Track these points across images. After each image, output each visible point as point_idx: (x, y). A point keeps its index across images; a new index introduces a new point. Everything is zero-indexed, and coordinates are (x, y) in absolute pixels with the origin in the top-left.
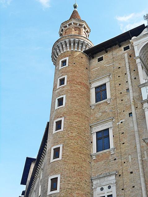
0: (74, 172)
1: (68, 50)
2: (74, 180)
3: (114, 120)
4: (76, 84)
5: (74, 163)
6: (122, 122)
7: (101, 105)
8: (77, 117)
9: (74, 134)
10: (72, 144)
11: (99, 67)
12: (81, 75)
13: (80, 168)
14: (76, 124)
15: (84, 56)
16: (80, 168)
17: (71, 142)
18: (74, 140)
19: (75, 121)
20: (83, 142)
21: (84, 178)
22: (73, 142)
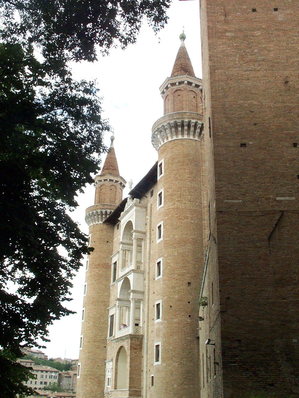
5: (89, 352)
8: (94, 306)
10: (88, 335)
15: (105, 226)
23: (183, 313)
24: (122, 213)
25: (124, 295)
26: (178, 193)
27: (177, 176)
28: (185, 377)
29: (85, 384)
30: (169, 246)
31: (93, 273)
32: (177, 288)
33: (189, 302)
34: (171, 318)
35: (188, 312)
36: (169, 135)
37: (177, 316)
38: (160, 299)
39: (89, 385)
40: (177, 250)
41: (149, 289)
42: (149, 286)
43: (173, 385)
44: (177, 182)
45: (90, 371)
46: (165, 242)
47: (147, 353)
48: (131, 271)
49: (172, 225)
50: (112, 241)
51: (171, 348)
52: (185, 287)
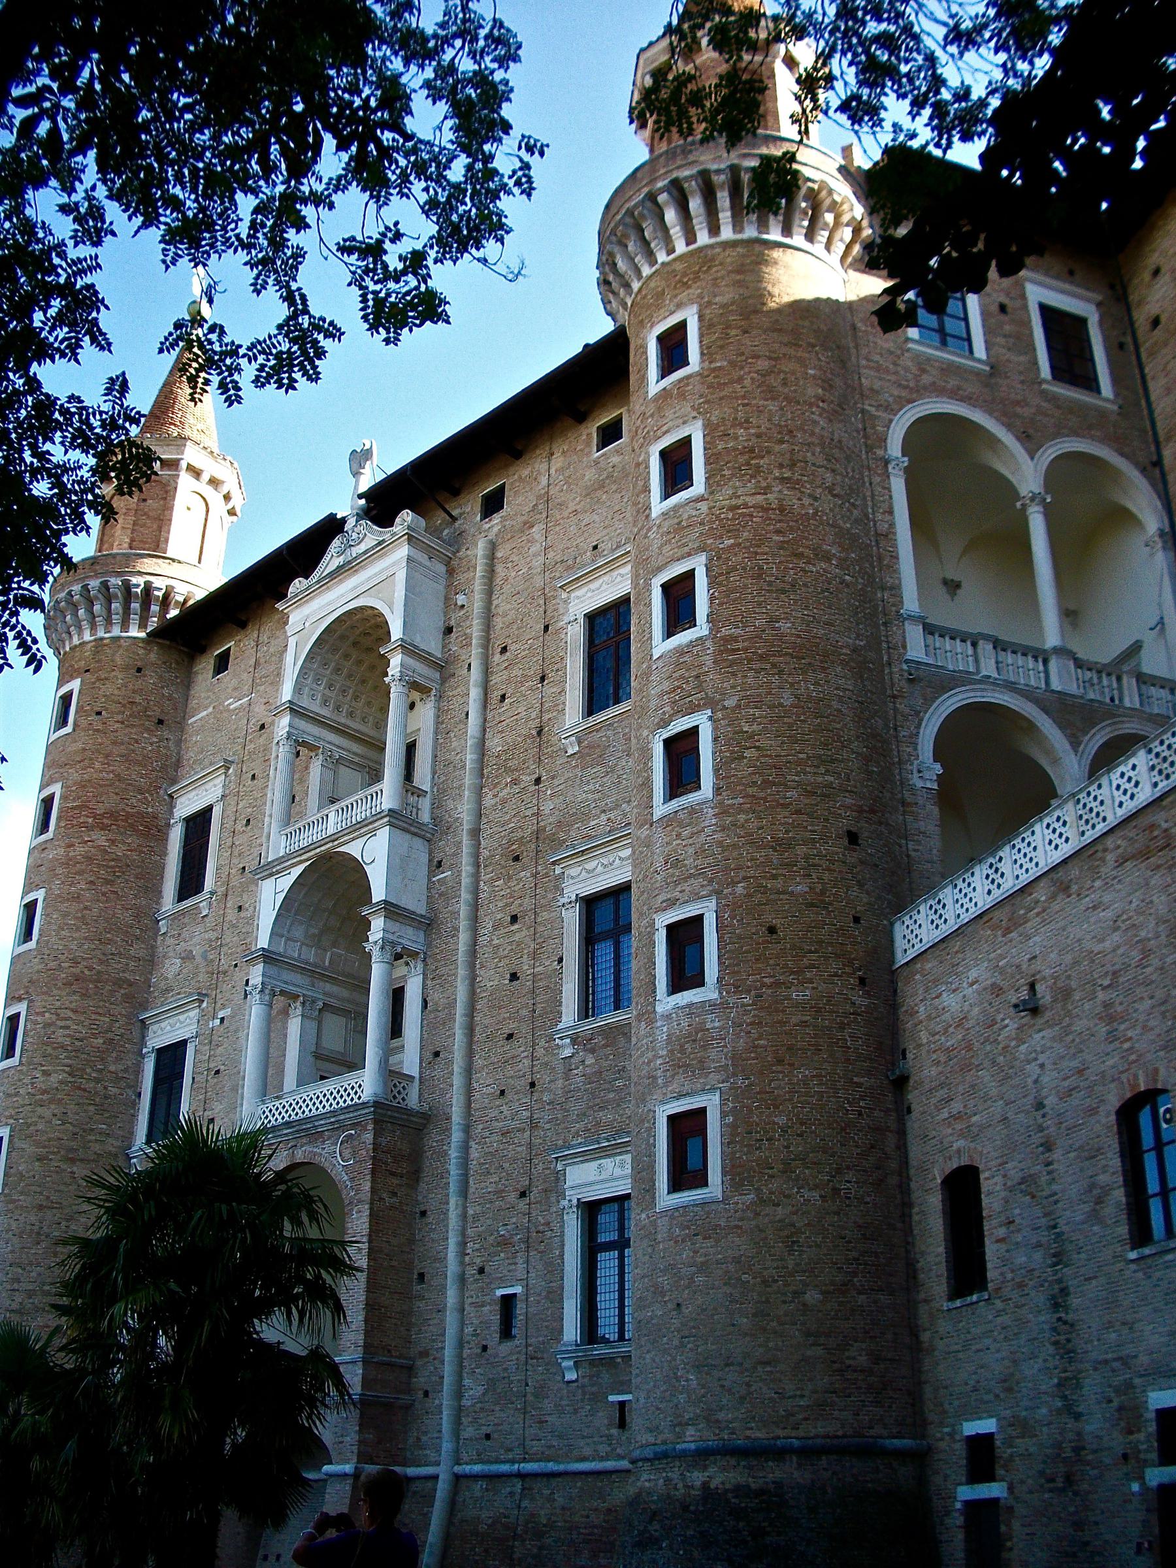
2: (33, 1274)
3: (205, 1005)
4: (90, 828)
6: (222, 1019)
7: (186, 920)
9: (54, 1078)
11: (211, 709)
13: (64, 1223)
14: (67, 1032)
16: (64, 1223)
17: (40, 1117)
18: (53, 1106)
20: (92, 1108)
23: (834, 966)
24: (297, 585)
25: (288, 939)
26: (777, 448)
27: (774, 381)
28: (855, 1254)
30: (750, 661)
31: (80, 850)
32: (801, 850)
33: (856, 920)
34: (777, 984)
35: (857, 964)
37: (808, 975)
38: (697, 897)
40: (792, 685)
41: (475, 906)
42: (475, 891)
44: (772, 406)
46: (724, 646)
47: (464, 1192)
48: (378, 816)
49: (760, 576)
50: (181, 725)
51: (782, 1120)
52: (836, 848)
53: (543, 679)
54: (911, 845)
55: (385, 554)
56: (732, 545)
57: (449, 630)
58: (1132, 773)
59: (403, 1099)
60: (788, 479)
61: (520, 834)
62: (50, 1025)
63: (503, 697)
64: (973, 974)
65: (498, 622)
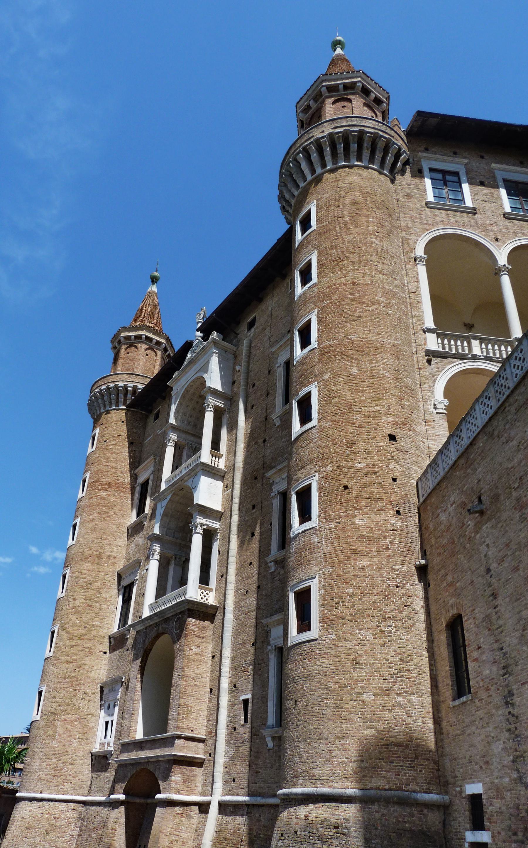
0: (65, 679)
1: (103, 410)
4: (100, 490)
5: (67, 662)
8: (90, 564)
9: (77, 602)
10: (70, 624)
12: (113, 464)
13: (77, 669)
14: (84, 580)
16: (77, 669)
19: (83, 575)
20: (94, 615)
21: (83, 688)
22: (74, 618)
25: (168, 529)
29: (50, 732)
36: (328, 158)
37: (365, 510)
39: (60, 735)
43: (358, 694)
45: (68, 704)
51: (350, 591)
53: (268, 395)
54: (430, 442)
55: (206, 353)
56: (329, 303)
57: (234, 382)
58: (521, 355)
59: (207, 600)
60: (357, 269)
61: (257, 467)
62: (77, 577)
63: (253, 406)
64: (452, 499)
65: (252, 374)
